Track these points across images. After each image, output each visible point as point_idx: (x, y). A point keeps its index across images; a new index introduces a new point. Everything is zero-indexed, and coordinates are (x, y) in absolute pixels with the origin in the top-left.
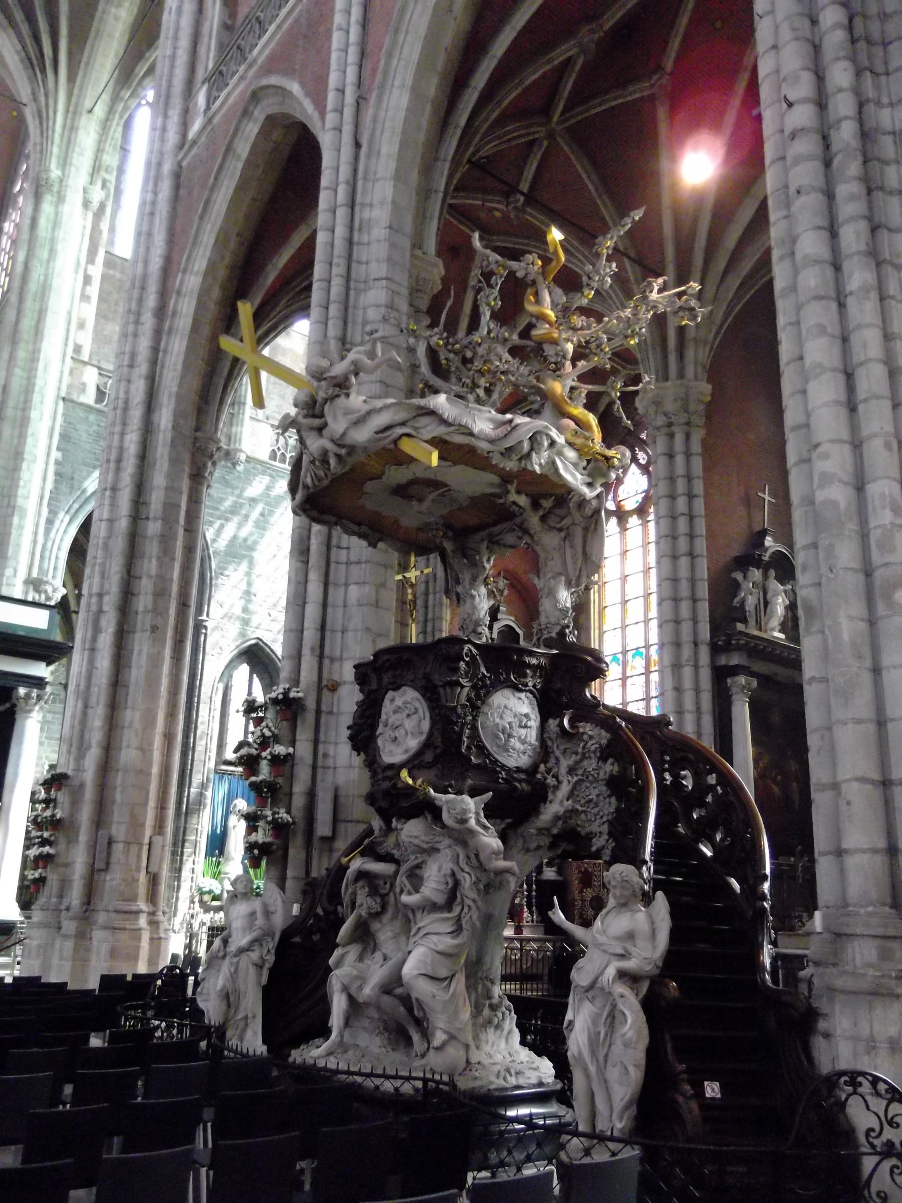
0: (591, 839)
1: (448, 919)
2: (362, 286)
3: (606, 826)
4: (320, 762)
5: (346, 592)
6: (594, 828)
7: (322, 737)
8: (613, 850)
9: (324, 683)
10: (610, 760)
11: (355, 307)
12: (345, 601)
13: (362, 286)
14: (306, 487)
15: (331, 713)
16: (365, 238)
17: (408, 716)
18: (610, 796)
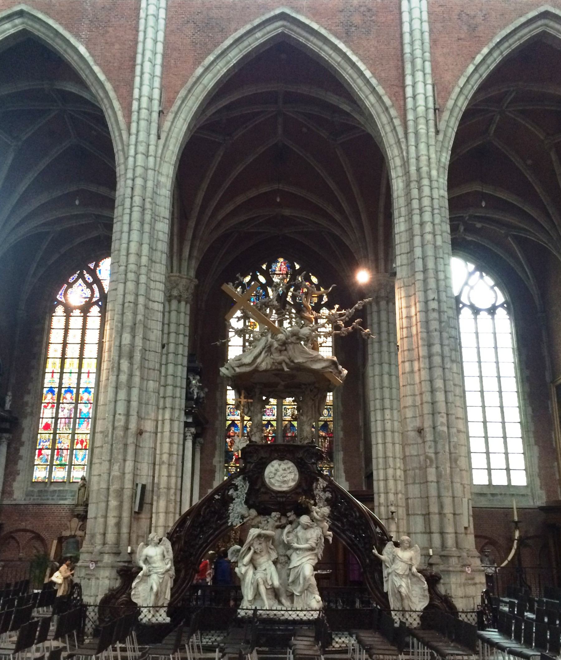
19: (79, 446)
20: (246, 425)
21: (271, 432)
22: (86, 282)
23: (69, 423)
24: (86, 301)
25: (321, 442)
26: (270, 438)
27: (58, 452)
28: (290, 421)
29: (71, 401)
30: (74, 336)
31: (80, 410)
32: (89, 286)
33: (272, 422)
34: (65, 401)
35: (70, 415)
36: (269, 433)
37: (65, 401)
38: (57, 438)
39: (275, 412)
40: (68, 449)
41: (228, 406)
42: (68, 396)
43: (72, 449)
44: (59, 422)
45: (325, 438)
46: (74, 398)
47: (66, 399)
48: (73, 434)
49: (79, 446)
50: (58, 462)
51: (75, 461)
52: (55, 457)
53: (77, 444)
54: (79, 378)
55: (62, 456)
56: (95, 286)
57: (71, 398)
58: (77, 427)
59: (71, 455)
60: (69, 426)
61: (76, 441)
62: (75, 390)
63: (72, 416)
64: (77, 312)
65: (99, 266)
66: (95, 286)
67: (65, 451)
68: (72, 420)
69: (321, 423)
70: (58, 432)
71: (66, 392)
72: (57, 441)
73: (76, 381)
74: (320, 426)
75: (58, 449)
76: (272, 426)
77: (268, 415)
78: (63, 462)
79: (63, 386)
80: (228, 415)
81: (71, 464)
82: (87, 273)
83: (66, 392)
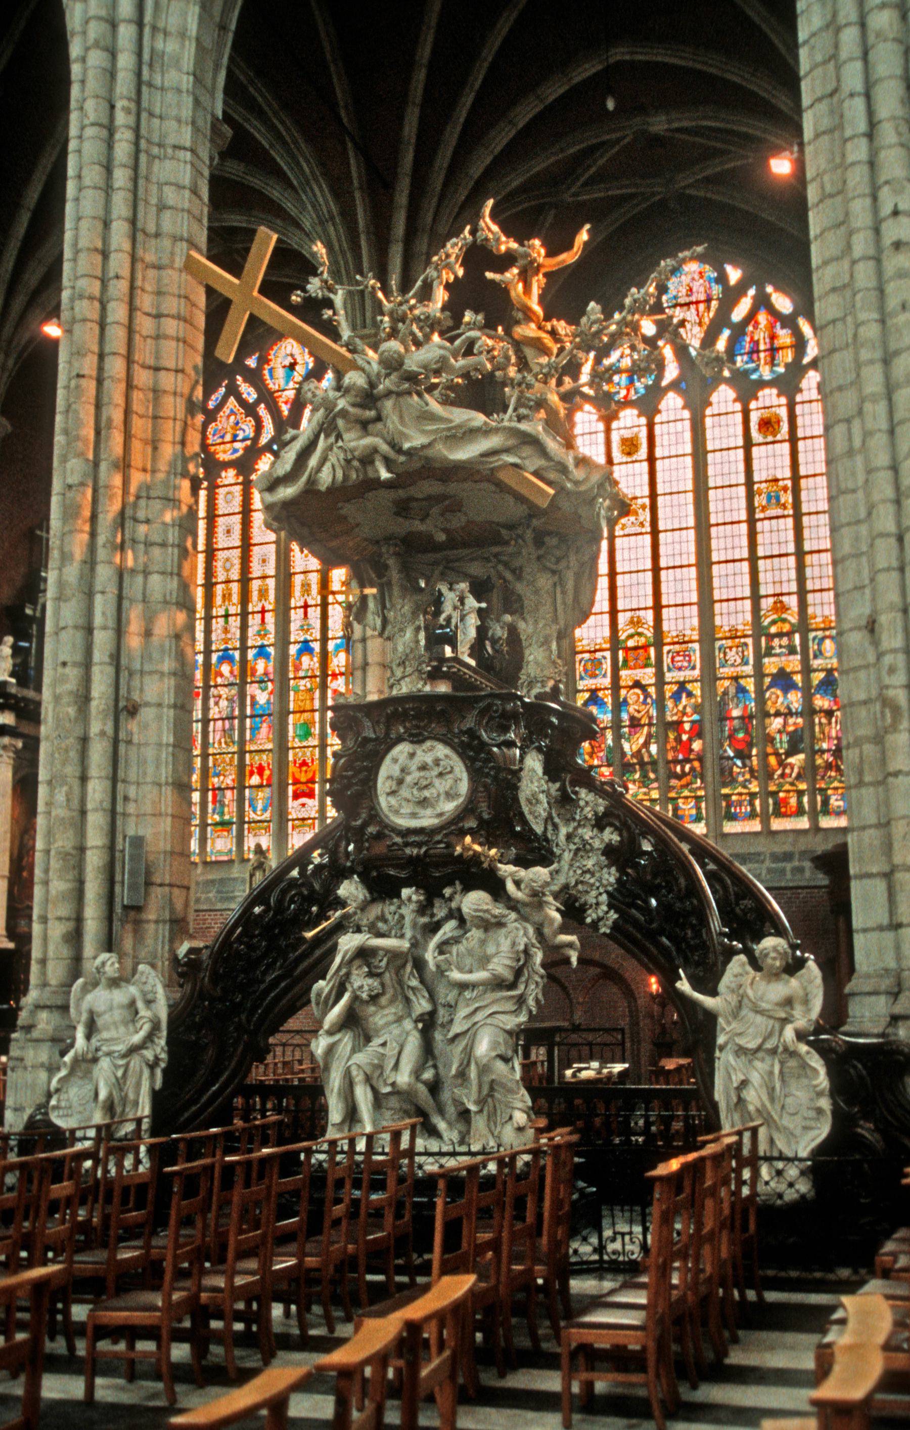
0: (585, 911)
1: (512, 997)
2: (155, 150)
3: (604, 898)
4: (119, 809)
5: (145, 584)
6: (591, 899)
7: (121, 774)
8: (615, 922)
9: (122, 704)
10: (608, 830)
11: (147, 179)
12: (144, 594)
13: (155, 150)
14: (312, 481)
15: (129, 742)
16: (158, 80)
17: (441, 775)
18: (609, 866)
19: (255, 780)
20: (625, 700)
21: (688, 710)
22: (242, 402)
23: (232, 728)
24: (246, 449)
25: (820, 724)
26: (687, 727)
27: (214, 796)
28: (736, 678)
29: (232, 680)
30: (228, 532)
31: (253, 698)
32: (250, 410)
33: (689, 686)
34: (219, 680)
35: (233, 710)
36: (684, 713)
37: (219, 680)
38: (211, 764)
39: (697, 658)
40: (232, 789)
41: (578, 657)
42: (225, 669)
43: (241, 787)
44: (211, 728)
45: (829, 713)
46: (236, 672)
47: (222, 675)
48: (242, 753)
49: (255, 780)
50: (217, 818)
51: (250, 815)
52: (210, 807)
53: (252, 773)
54: (244, 627)
55: (223, 805)
56: (262, 410)
57: (231, 672)
58: (248, 737)
59: (241, 800)
60: (231, 737)
61: (248, 769)
62: (237, 655)
63: (237, 713)
64: (229, 476)
65: (268, 362)
66: (262, 410)
67: (228, 793)
68: (236, 722)
69: (820, 676)
70: (211, 751)
71: (221, 660)
72: (211, 771)
73: (238, 635)
74: (815, 682)
75: (214, 789)
76: (690, 695)
77: (680, 669)
78: (227, 817)
79: (214, 648)
80: (582, 678)
81: (241, 822)
82: (245, 381)
83: (221, 660)
